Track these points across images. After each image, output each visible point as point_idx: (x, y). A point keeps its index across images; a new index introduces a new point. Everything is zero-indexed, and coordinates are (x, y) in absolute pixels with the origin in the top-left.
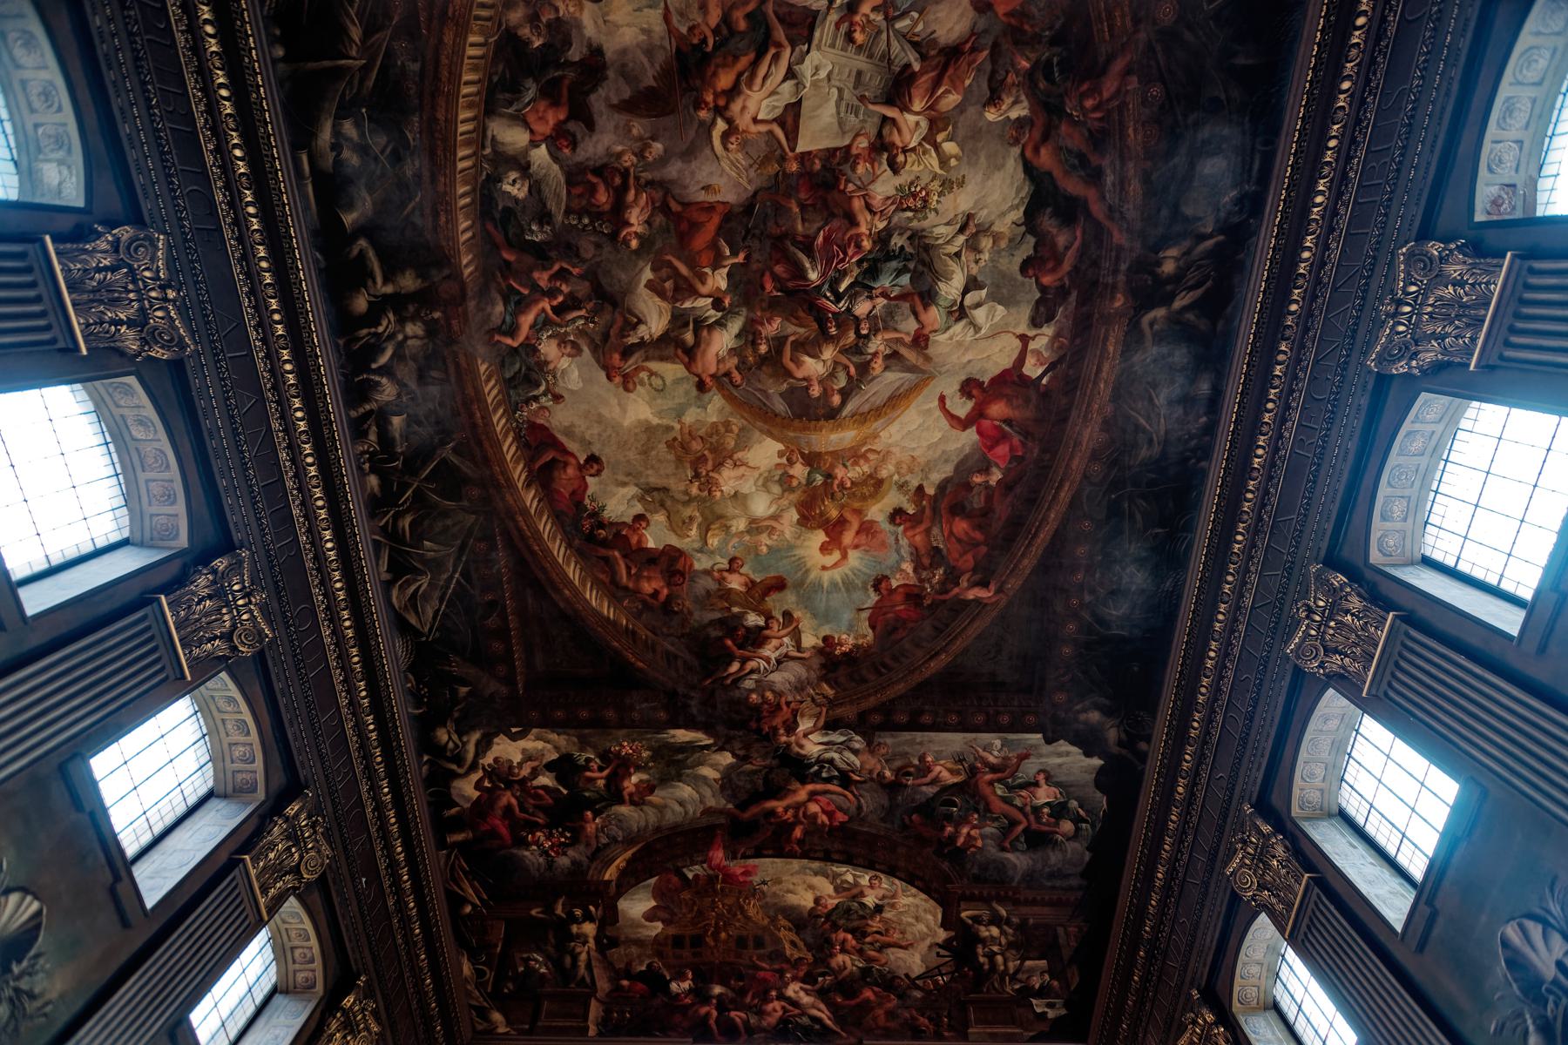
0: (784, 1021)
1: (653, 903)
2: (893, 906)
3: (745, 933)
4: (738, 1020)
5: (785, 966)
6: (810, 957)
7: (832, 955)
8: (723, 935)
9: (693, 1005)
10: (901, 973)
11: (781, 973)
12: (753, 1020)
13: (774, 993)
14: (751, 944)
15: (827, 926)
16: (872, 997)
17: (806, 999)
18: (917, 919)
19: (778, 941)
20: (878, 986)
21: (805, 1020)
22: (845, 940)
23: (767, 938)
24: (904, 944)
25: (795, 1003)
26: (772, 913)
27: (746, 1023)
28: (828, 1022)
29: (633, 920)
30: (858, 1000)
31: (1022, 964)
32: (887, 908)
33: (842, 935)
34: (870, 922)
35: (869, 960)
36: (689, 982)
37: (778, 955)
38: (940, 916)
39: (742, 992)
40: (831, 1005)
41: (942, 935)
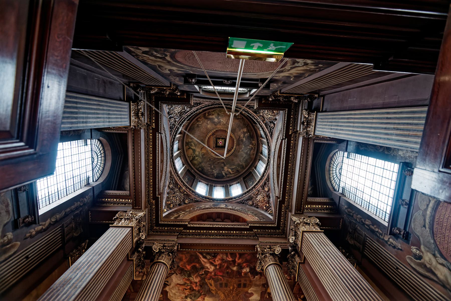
0: (215, 257)
1: (250, 298)
2: (182, 298)
3: (225, 289)
4: (230, 257)
5: (214, 277)
6: (206, 280)
7: (200, 281)
8: (231, 288)
9: (243, 263)
10: (179, 275)
11: (215, 275)
12: (225, 257)
13: (218, 267)
14: (224, 285)
15: (201, 291)
16: (187, 266)
17: (208, 265)
18: (175, 294)
19: (216, 286)
20: (186, 271)
21: (208, 257)
22: (196, 286)
23: (219, 286)
24: (178, 286)
25: (211, 264)
26: (217, 295)
27: (227, 256)
28: (201, 256)
29: (257, 293)
30: (192, 265)
31: (142, 279)
32: (184, 297)
33: (197, 289)
34: (189, 293)
35: (189, 280)
36: (243, 272)
37: (216, 281)
38: (168, 295)
39: (228, 267)
40: (199, 262)
41: (167, 289)
